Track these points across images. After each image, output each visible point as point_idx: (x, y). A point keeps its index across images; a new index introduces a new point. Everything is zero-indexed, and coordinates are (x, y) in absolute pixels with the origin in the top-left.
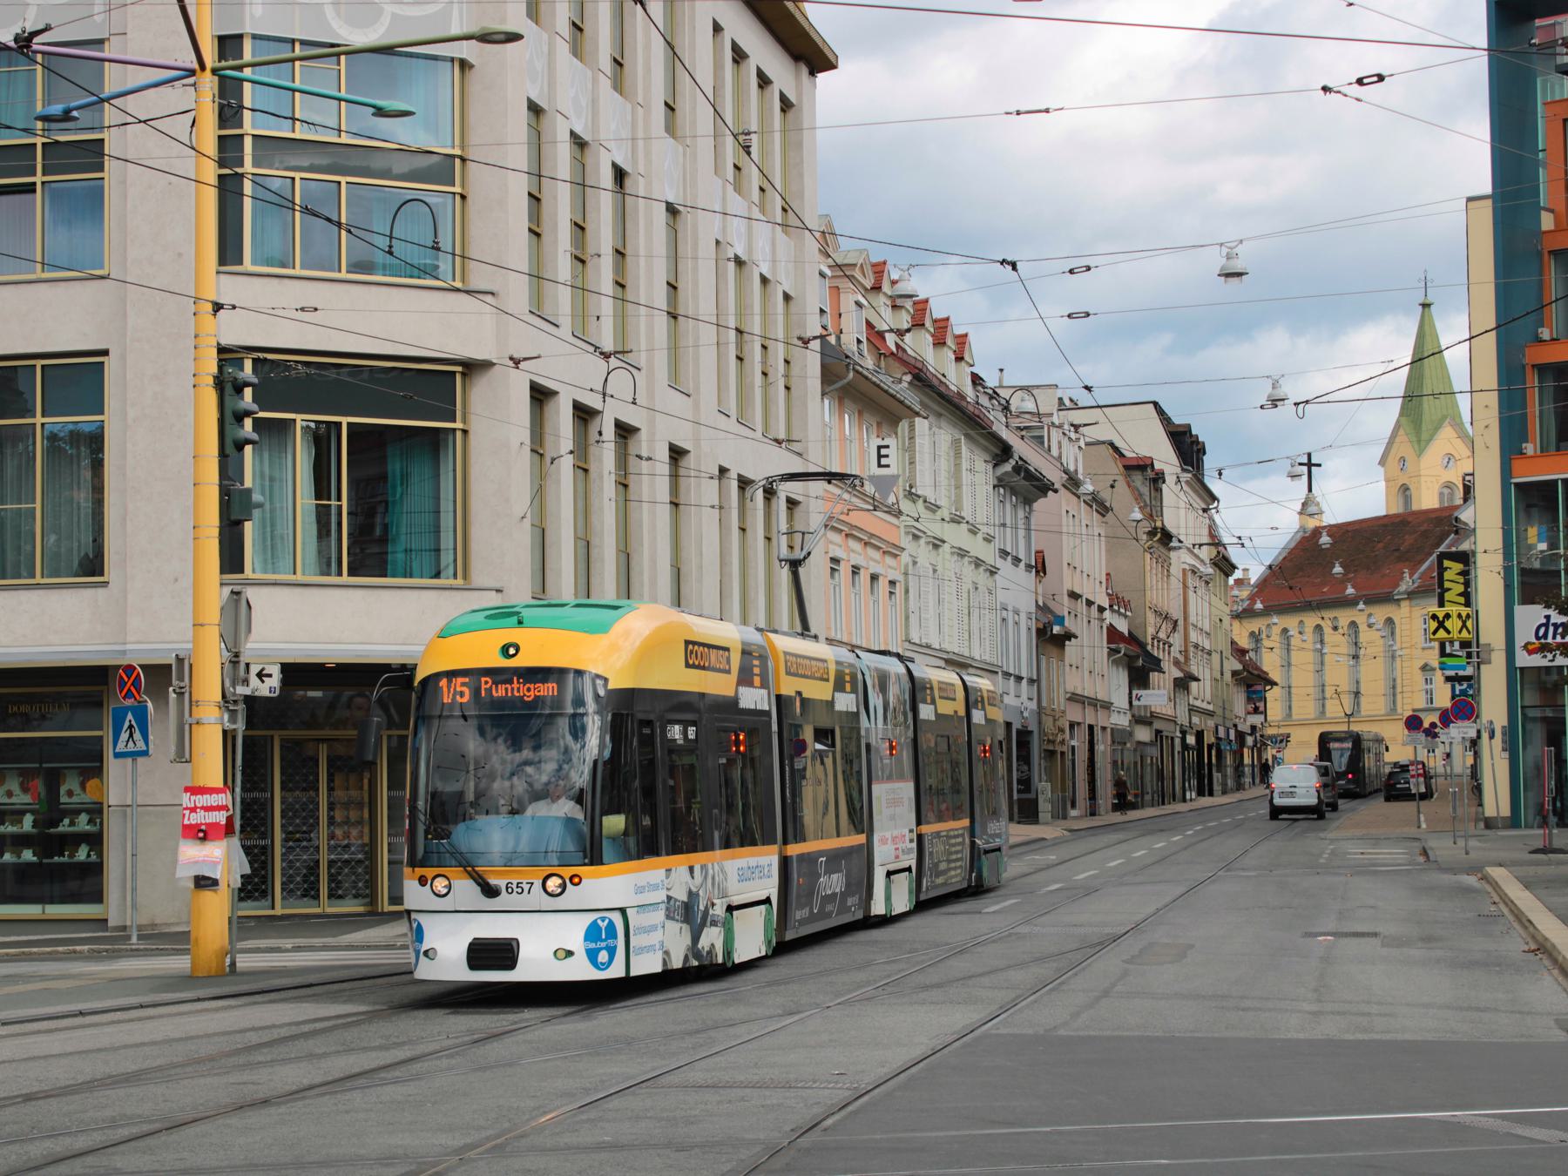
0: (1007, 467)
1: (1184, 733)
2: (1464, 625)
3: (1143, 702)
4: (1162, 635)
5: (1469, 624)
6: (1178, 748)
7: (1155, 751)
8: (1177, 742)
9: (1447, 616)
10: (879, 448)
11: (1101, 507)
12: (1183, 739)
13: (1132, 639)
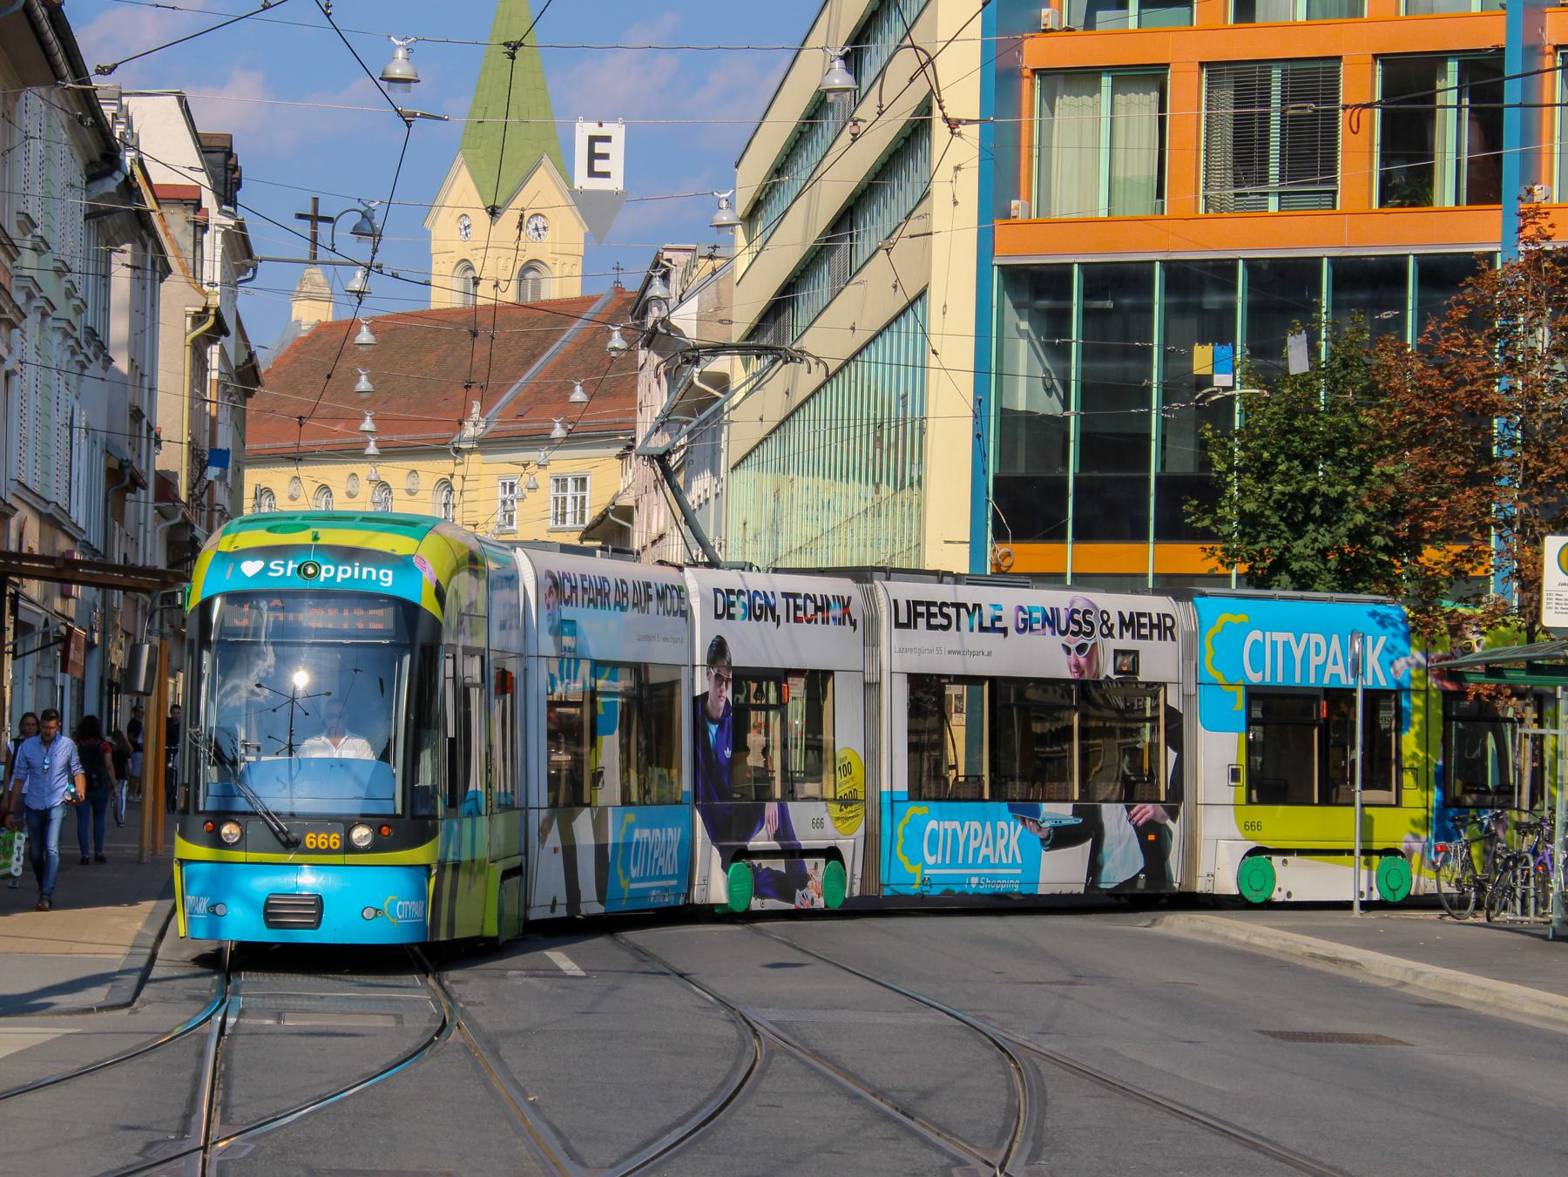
10: (593, 140)
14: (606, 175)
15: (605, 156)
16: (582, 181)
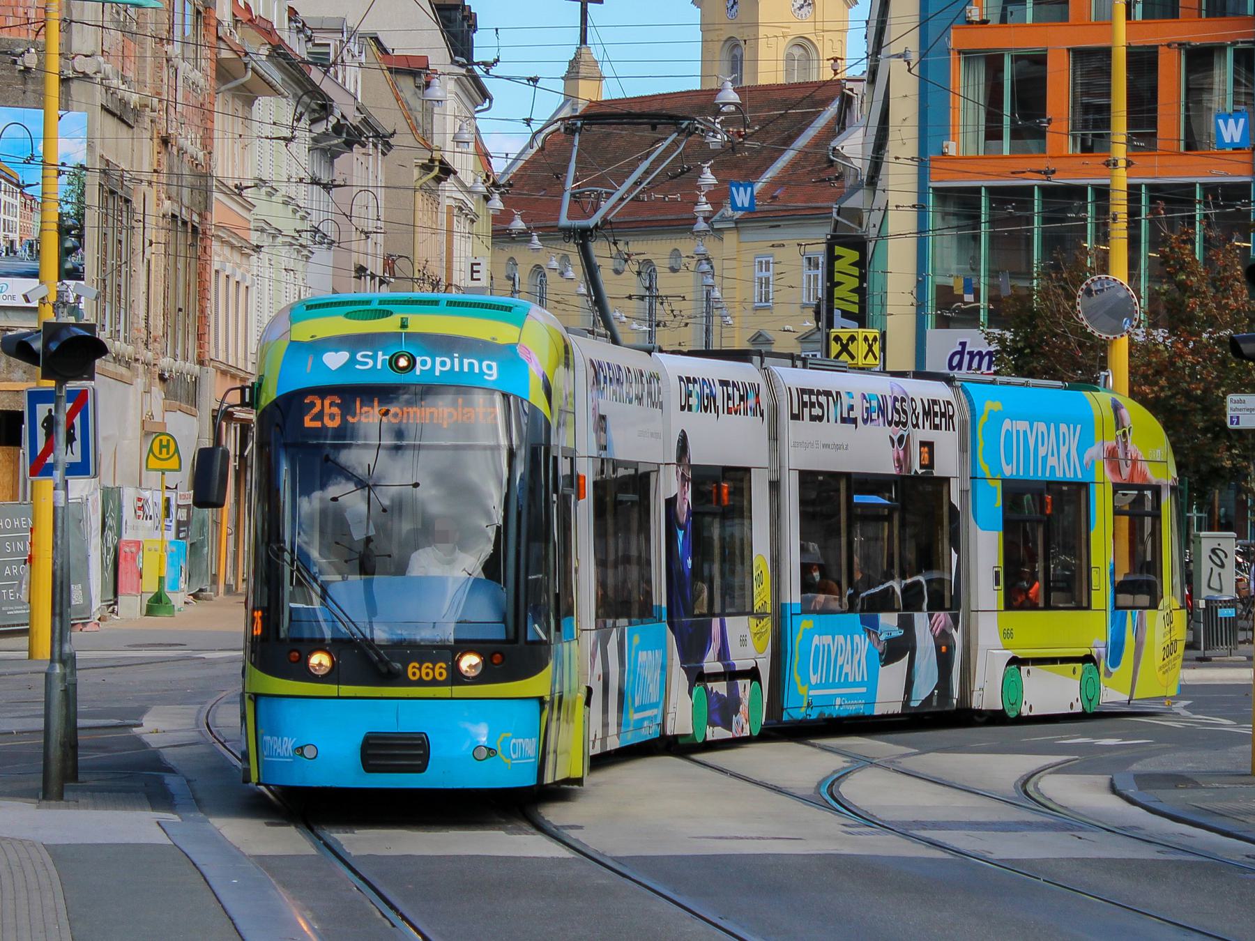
2: (870, 349)
5: (876, 348)
9: (852, 339)
10: (473, 265)
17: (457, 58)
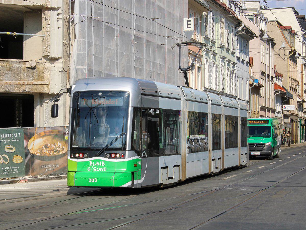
0: (240, 29)
1: (301, 120)
3: (286, 109)
4: (294, 87)
6: (299, 125)
7: (289, 126)
8: (298, 123)
10: (188, 21)
11: (271, 42)
12: (300, 122)
13: (283, 87)
14: (190, 28)
15: (190, 24)
16: (186, 29)
17: (303, 30)
